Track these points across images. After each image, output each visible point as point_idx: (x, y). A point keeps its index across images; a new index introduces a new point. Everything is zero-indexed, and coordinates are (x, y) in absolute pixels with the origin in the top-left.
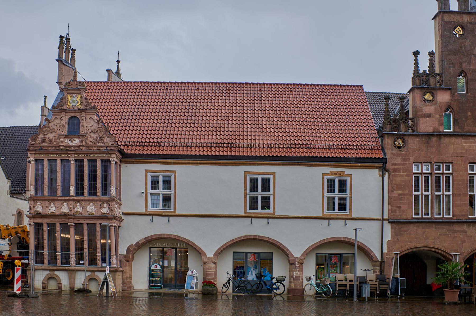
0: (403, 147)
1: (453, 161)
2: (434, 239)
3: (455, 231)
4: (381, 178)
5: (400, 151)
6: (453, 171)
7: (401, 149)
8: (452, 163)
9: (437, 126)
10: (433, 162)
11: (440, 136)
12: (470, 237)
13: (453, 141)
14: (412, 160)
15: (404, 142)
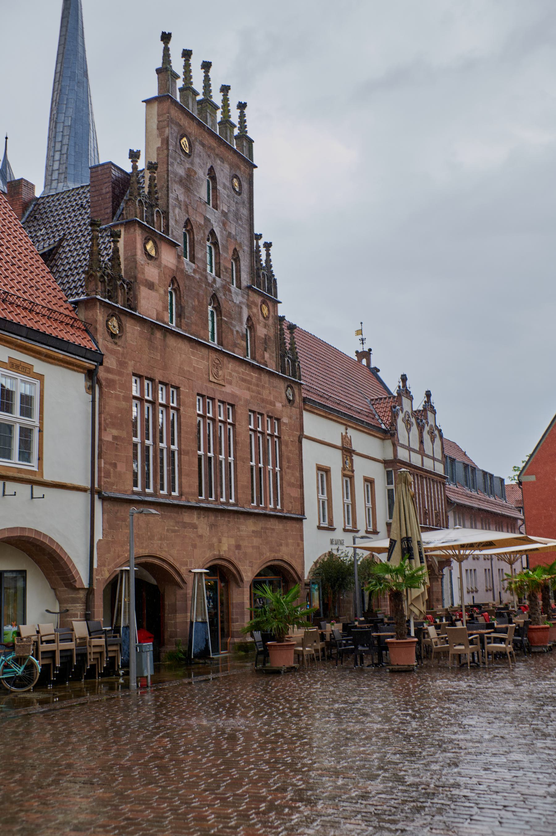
0: (119, 337)
1: (180, 386)
2: (161, 539)
3: (185, 525)
4: (91, 396)
5: (116, 344)
6: (179, 403)
7: (116, 341)
8: (177, 388)
9: (160, 309)
10: (157, 381)
11: (167, 331)
12: (201, 537)
13: (179, 345)
14: (130, 370)
15: (121, 327)
